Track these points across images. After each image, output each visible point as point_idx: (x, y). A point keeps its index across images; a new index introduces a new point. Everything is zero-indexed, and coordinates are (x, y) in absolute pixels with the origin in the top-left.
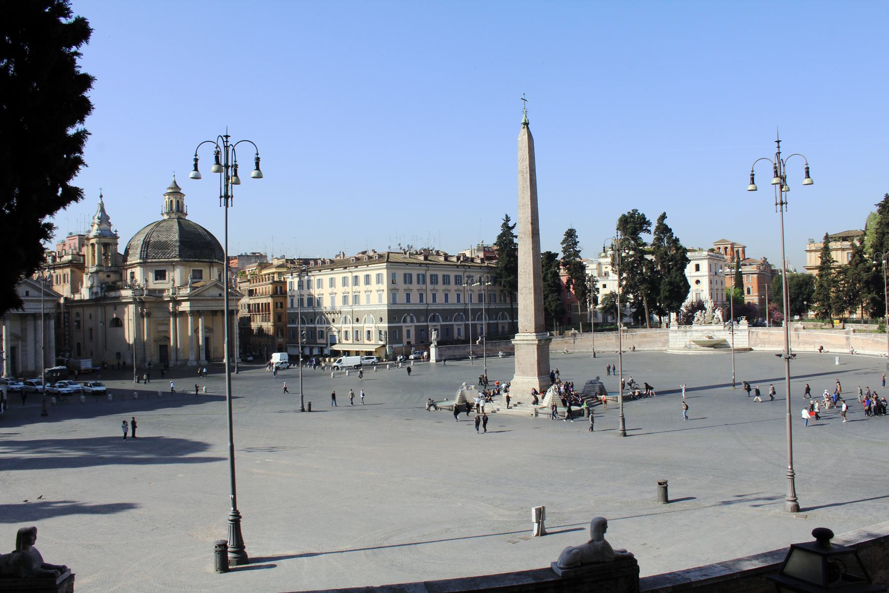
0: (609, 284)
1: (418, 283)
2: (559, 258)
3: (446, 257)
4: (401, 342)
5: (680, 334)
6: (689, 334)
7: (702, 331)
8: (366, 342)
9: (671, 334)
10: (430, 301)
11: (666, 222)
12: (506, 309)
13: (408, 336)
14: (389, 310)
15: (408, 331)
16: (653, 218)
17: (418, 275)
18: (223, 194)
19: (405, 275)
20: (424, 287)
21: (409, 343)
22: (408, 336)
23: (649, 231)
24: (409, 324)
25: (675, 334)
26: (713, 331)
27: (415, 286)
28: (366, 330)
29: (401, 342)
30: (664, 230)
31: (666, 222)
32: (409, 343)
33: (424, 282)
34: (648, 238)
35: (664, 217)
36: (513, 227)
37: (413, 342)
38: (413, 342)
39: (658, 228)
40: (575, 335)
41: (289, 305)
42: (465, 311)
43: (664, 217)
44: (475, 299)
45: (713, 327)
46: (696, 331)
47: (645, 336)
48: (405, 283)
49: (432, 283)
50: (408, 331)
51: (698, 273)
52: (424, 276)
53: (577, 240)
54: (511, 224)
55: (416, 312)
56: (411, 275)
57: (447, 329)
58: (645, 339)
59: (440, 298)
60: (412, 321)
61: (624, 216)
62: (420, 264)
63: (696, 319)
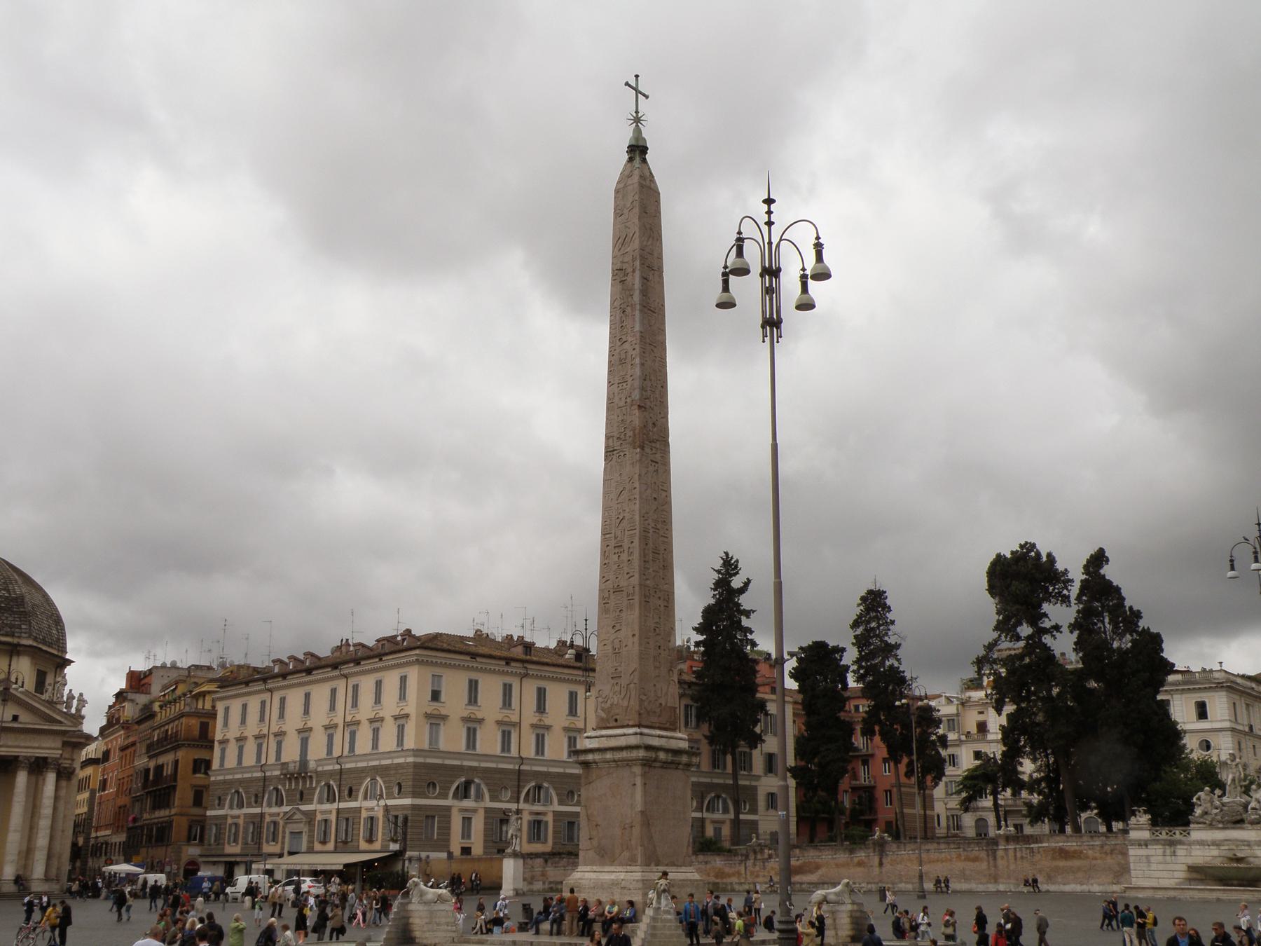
0: (975, 726)
5: (1156, 851)
6: (1181, 850)
7: (1216, 844)
8: (363, 845)
9: (1133, 851)
10: (529, 751)
11: (1108, 571)
12: (724, 787)
13: (466, 833)
16: (1072, 564)
21: (466, 851)
22: (466, 833)
23: (1065, 600)
24: (468, 803)
25: (1143, 852)
26: (1248, 844)
28: (364, 814)
32: (466, 851)
35: (1098, 559)
36: (742, 590)
37: (478, 849)
38: (478, 849)
39: (1085, 586)
41: (215, 765)
46: (1202, 843)
47: (1064, 854)
50: (467, 821)
53: (890, 616)
58: (1062, 863)
60: (479, 797)
61: (999, 559)
63: (1198, 811)
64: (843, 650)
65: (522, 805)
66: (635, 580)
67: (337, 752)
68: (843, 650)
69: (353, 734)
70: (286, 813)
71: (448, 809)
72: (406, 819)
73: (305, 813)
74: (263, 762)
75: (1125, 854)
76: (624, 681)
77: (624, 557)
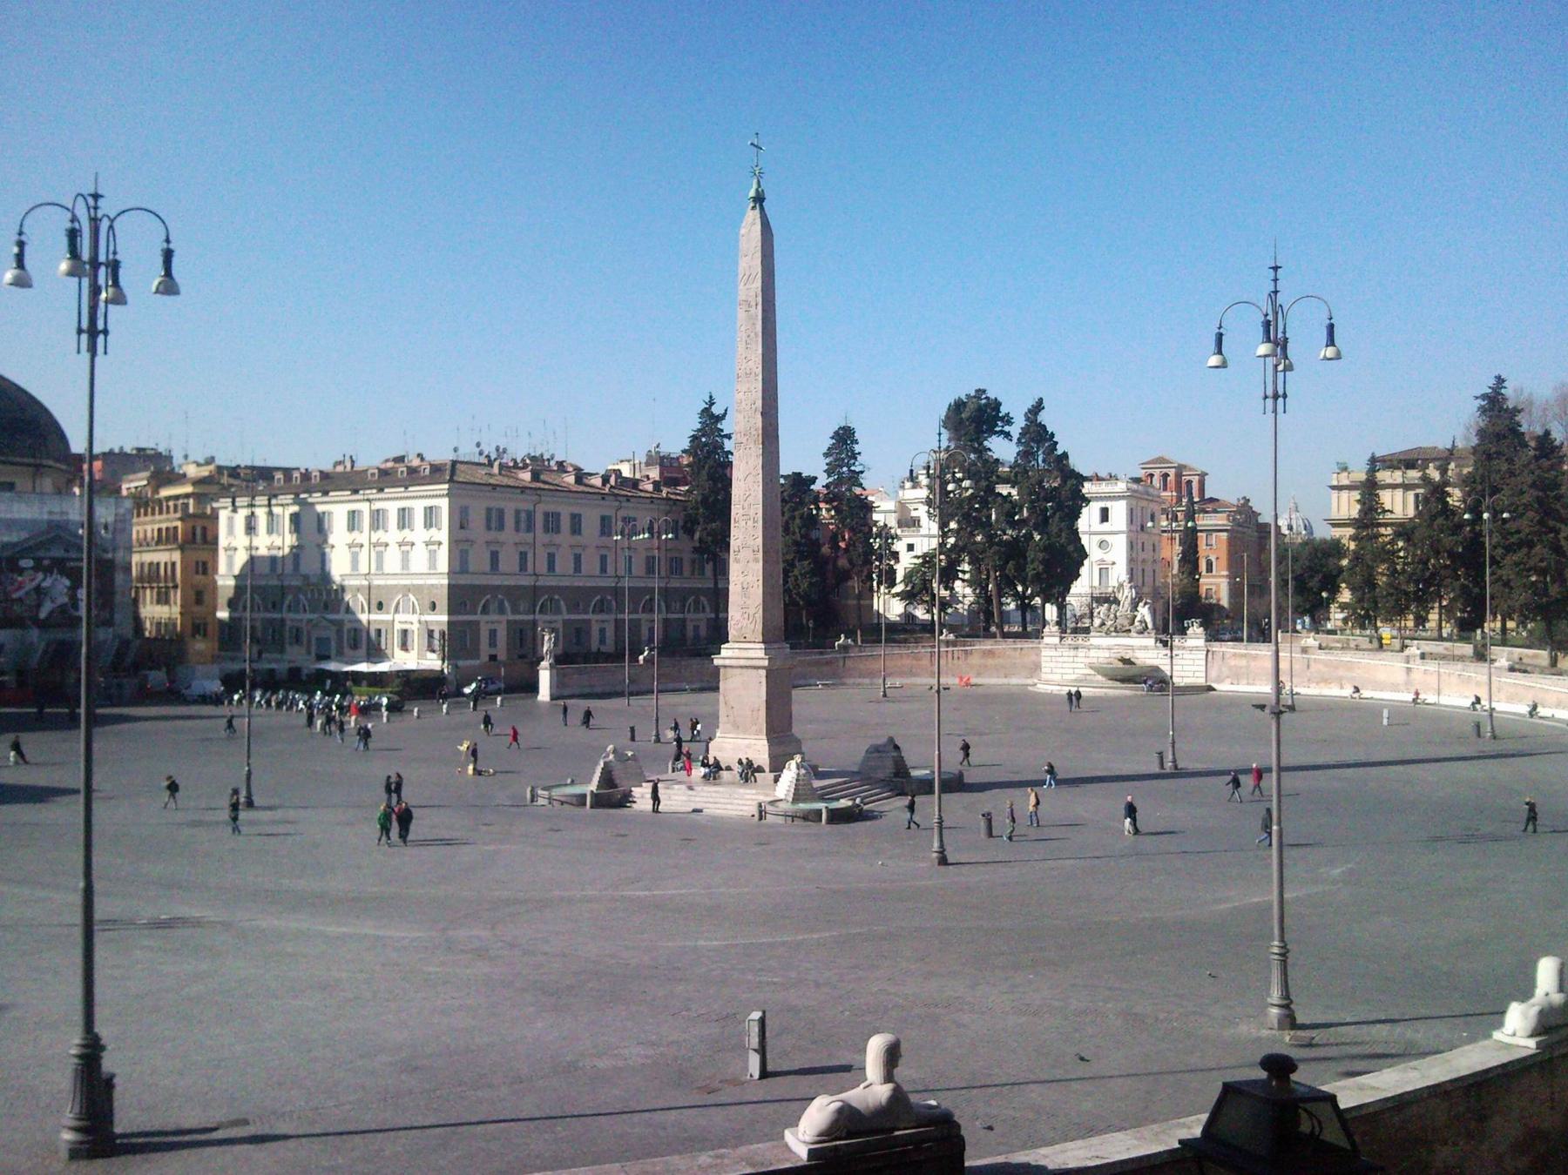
1: (517, 530)
2: (817, 487)
3: (581, 476)
4: (478, 657)
6: (1081, 653)
10: (542, 567)
11: (1043, 418)
13: (493, 643)
14: (450, 586)
15: (493, 633)
16: (1015, 408)
17: (517, 512)
18: (101, 338)
19: (489, 510)
20: (529, 537)
21: (493, 658)
22: (493, 643)
23: (1008, 435)
25: (1053, 653)
26: (1132, 648)
27: (509, 535)
28: (398, 627)
29: (478, 657)
30: (1037, 435)
31: (1043, 418)
32: (493, 658)
33: (530, 527)
34: (1003, 450)
35: (1038, 407)
37: (502, 656)
38: (502, 656)
39: (1025, 432)
40: (845, 648)
42: (617, 592)
43: (1038, 407)
44: (639, 567)
45: (1135, 641)
46: (1099, 648)
47: (991, 653)
48: (489, 528)
49: (546, 530)
50: (493, 633)
51: (1106, 527)
52: (530, 516)
53: (857, 448)
54: (717, 410)
55: (510, 591)
56: (501, 513)
57: (578, 631)
58: (990, 662)
59: (564, 564)
60: (502, 611)
62: (523, 489)
64: (813, 480)
65: (538, 616)
66: (760, 541)
67: (363, 569)
68: (813, 480)
69: (380, 556)
70: (310, 621)
71: (477, 623)
72: (442, 634)
73: (332, 622)
74: (279, 571)
75: (1038, 655)
76: (752, 611)
77: (750, 523)
